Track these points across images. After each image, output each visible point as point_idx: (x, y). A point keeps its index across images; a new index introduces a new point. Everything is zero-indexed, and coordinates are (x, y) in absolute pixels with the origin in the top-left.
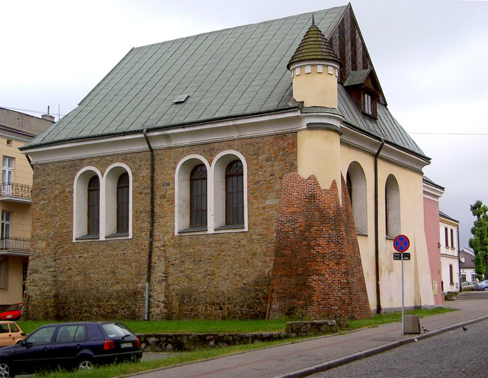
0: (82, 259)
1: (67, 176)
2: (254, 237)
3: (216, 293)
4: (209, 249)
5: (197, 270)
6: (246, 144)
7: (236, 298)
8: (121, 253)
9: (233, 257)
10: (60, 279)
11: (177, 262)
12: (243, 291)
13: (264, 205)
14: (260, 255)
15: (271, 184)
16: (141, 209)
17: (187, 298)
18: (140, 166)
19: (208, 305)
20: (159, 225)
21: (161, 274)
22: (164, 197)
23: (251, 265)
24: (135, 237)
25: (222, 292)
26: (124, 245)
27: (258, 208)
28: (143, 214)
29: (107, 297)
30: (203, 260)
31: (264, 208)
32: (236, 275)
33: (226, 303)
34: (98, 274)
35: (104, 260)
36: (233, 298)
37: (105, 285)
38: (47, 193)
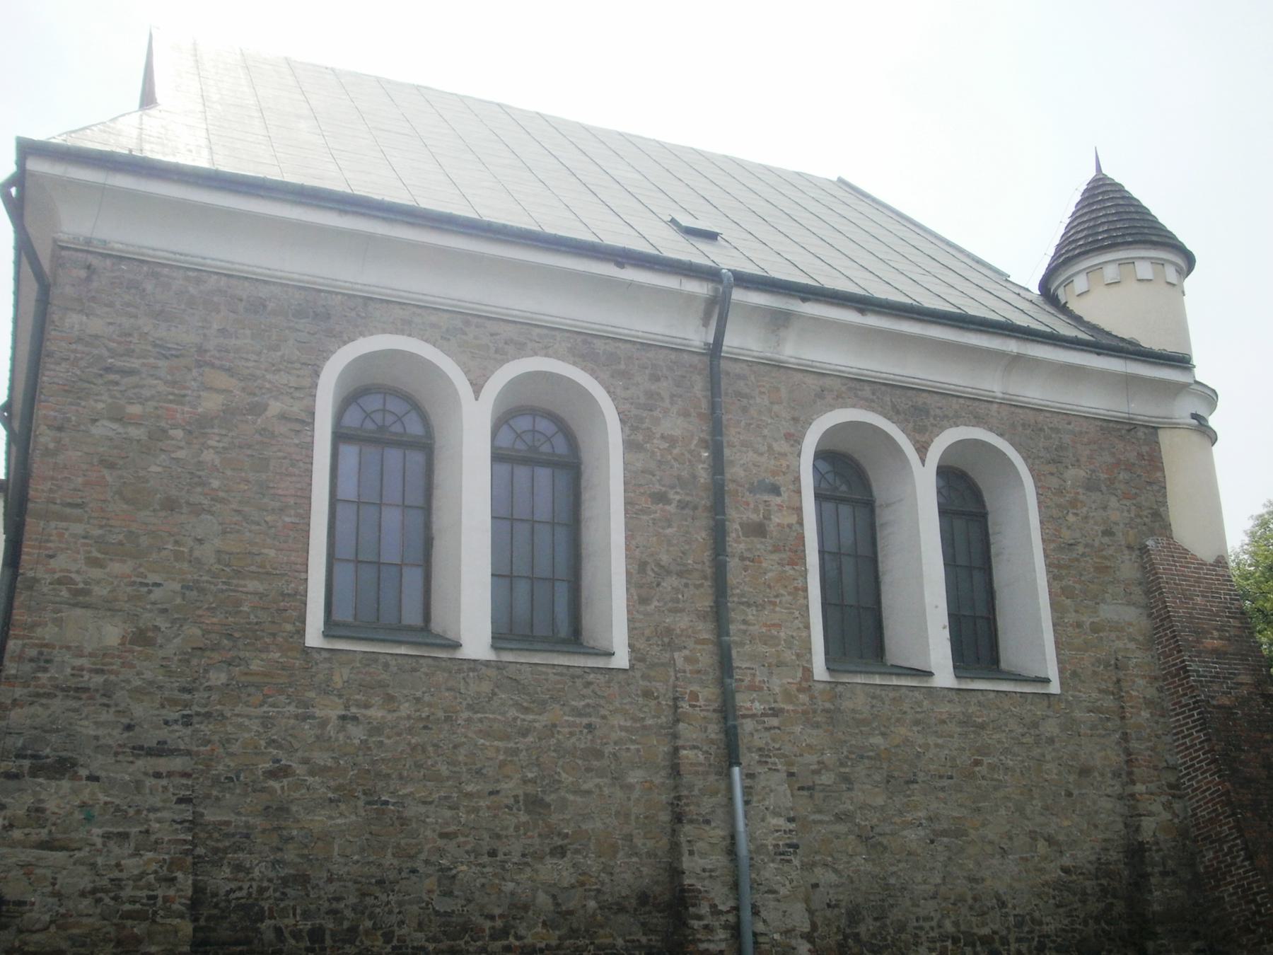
0: (357, 733)
1: (276, 348)
2: (1077, 714)
3: (975, 899)
4: (940, 741)
5: (901, 813)
6: (1029, 426)
7: (1044, 920)
8: (573, 725)
9: (1022, 774)
11: (826, 778)
12: (1065, 893)
13: (1096, 620)
14: (1102, 775)
15: (1106, 558)
16: (665, 559)
17: (870, 921)
18: (650, 395)
19: (949, 943)
20: (745, 632)
21: (780, 822)
22: (758, 530)
23: (1078, 806)
24: (639, 665)
25: (998, 897)
26: (585, 691)
27: (1079, 625)
28: (670, 582)
29: (497, 911)
30: (921, 777)
31: (1095, 628)
32: (1033, 836)
33: (1012, 938)
34: (453, 807)
35: (484, 748)
36: (1033, 920)
37: (486, 859)
38: (146, 393)
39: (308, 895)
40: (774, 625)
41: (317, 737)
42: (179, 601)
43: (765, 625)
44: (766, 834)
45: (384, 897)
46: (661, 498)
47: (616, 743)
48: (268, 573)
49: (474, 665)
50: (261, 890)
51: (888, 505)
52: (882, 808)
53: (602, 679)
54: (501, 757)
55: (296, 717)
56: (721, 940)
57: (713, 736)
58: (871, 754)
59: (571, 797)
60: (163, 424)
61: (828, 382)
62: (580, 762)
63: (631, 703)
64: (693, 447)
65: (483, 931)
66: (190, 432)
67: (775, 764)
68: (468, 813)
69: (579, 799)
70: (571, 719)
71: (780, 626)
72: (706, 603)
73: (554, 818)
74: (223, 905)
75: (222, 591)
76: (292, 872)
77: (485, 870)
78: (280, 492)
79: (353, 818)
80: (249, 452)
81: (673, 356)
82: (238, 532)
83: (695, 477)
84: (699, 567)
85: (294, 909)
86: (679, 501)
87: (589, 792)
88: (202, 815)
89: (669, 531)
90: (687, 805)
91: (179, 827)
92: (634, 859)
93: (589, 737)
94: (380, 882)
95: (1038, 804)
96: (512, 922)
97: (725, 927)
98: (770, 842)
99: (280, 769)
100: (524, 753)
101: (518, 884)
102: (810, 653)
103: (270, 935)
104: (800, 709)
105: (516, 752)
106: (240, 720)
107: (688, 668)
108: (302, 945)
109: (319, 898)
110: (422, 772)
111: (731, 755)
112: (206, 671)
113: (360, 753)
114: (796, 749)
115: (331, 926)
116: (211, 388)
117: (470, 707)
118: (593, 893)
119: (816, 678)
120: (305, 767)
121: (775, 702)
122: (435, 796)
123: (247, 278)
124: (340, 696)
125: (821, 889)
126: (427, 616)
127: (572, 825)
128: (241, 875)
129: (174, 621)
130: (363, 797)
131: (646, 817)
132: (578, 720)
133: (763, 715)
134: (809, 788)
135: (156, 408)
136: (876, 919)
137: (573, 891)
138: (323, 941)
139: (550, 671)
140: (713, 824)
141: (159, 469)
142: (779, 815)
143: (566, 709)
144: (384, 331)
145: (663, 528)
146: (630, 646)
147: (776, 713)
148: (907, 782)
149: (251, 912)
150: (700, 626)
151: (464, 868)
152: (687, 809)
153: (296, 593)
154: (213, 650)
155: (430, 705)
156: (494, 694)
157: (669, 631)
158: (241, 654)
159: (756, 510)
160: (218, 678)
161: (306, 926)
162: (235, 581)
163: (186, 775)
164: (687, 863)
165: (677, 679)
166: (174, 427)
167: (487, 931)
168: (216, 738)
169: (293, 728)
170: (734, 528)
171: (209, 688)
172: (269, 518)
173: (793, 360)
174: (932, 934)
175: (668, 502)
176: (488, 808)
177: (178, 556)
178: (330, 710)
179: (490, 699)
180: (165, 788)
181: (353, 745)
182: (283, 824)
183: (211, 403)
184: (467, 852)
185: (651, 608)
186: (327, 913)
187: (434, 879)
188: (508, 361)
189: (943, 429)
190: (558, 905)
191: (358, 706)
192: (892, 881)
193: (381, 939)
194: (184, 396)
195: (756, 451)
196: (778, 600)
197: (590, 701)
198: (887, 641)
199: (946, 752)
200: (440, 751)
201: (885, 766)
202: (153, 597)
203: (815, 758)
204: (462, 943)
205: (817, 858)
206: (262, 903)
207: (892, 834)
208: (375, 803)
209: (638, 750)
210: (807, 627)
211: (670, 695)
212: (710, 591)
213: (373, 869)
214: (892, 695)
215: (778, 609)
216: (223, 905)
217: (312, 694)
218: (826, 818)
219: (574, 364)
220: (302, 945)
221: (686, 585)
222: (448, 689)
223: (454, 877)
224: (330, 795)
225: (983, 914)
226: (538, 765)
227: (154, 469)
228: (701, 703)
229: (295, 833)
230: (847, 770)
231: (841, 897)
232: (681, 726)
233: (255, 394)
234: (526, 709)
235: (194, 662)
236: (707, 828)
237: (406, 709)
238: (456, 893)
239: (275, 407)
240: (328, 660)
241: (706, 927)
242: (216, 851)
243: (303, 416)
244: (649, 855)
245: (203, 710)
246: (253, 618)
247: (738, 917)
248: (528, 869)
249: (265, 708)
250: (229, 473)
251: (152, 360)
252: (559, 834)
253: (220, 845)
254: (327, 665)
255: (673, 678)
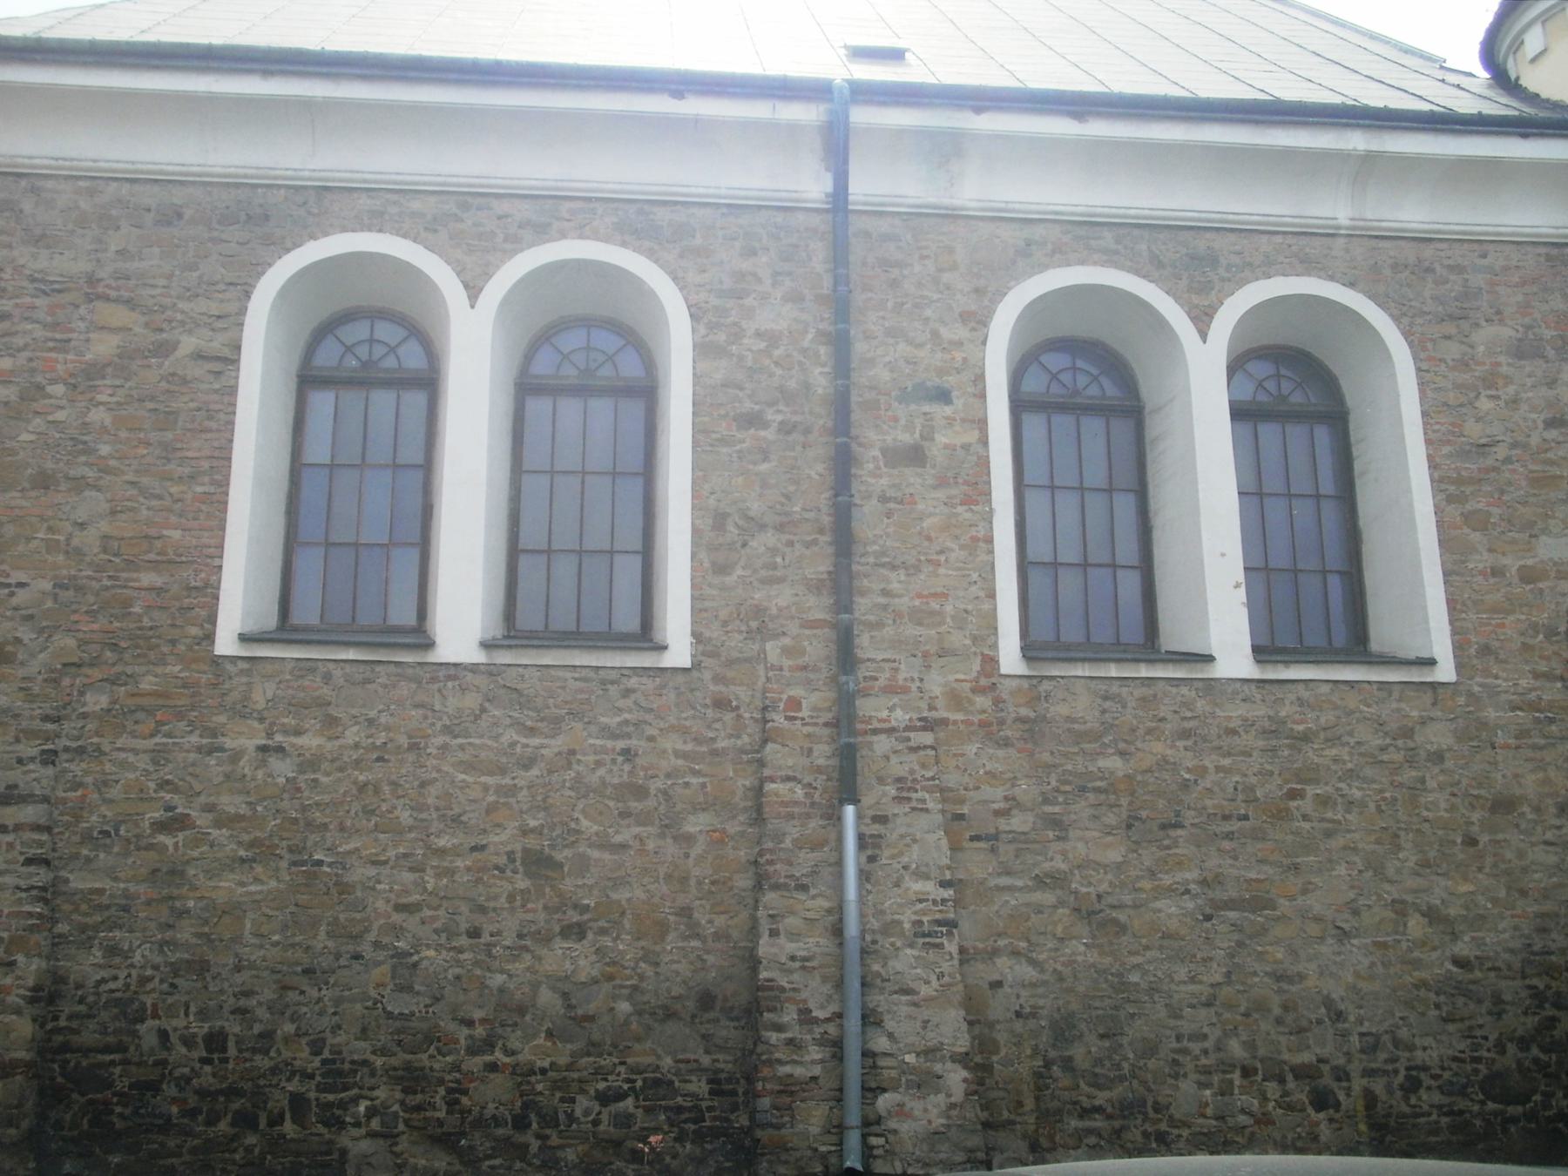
0: (282, 768)
1: (193, 267)
2: (1491, 714)
3: (1286, 1008)
4: (1226, 762)
5: (1152, 874)
7: (1417, 1041)
8: (604, 750)
9: (1379, 810)
10: (78, 881)
11: (1019, 822)
12: (1460, 1001)
13: (1530, 562)
14: (1537, 810)
15: (1552, 463)
16: (755, 507)
17: (1092, 1039)
18: (741, 276)
19: (1236, 1077)
20: (885, 607)
21: (929, 887)
22: (915, 456)
23: (1489, 860)
24: (707, 662)
25: (1328, 1003)
26: (621, 703)
27: (1497, 572)
29: (478, 1014)
30: (1190, 817)
31: (1528, 576)
32: (1400, 909)
33: (1355, 1068)
34: (418, 869)
35: (465, 786)
36: (1397, 1043)
37: (463, 941)
38: (19, 341)
39: (206, 988)
40: (935, 595)
41: (227, 776)
42: (49, 604)
43: (919, 596)
44: (901, 905)
45: (314, 993)
46: (752, 420)
47: (668, 776)
48: (170, 562)
49: (455, 670)
50: (144, 980)
51: (1160, 408)
52: (1119, 866)
53: (650, 684)
54: (491, 798)
55: (199, 749)
56: (813, 1062)
57: (821, 762)
58: (1099, 784)
59: (595, 854)
60: (39, 379)
61: (1039, 232)
62: (611, 804)
63: (694, 717)
64: (806, 344)
65: (457, 1041)
66: (75, 386)
67: (924, 801)
68: (438, 876)
69: (607, 856)
70: (598, 742)
71: (945, 596)
72: (820, 565)
73: (568, 885)
74: (91, 999)
75: (107, 588)
76: (186, 956)
77: (462, 957)
78: (190, 454)
79: (273, 884)
80: (151, 405)
81: (779, 218)
82: (132, 509)
83: (807, 386)
84: (811, 515)
85: (187, 1008)
86: (781, 423)
87: (624, 847)
88: (67, 881)
89: (764, 467)
90: (771, 863)
91: (24, 895)
92: (695, 943)
93: (627, 767)
94: (308, 972)
95: (1409, 857)
96: (499, 1031)
97: (822, 1042)
98: (907, 918)
99: (174, 819)
100: (525, 792)
101: (510, 976)
102: (996, 634)
103: (150, 1040)
104: (975, 719)
105: (513, 790)
106: (123, 755)
107: (787, 663)
108: (196, 1055)
109: (222, 991)
110: (374, 820)
111: (847, 787)
112: (82, 693)
113: (286, 796)
114: (966, 779)
115: (237, 1029)
116: (102, 328)
117: (447, 730)
118: (625, 992)
119: (1003, 671)
120: (210, 816)
121: (931, 708)
122: (391, 853)
123: (156, 181)
124: (261, 720)
125: (1007, 989)
126: (422, 612)
127: (595, 892)
128: (117, 960)
129: (41, 631)
130: (287, 856)
131: (713, 883)
132: (609, 744)
133: (907, 728)
134: (988, 838)
135: (31, 360)
136: (1102, 1036)
137: (595, 987)
138: (224, 1049)
139: (568, 675)
140: (813, 892)
141: (33, 437)
142: (927, 877)
143: (593, 728)
144: (344, 229)
145: (755, 463)
146: (693, 634)
147: (928, 725)
148: (1163, 827)
149: (129, 1010)
150: (812, 600)
151: (431, 953)
152: (771, 869)
153: (207, 585)
154: (92, 665)
155: (388, 729)
156: (483, 710)
157: (759, 611)
158: (129, 670)
159: (909, 428)
160: (97, 701)
161: (200, 1029)
162: (124, 575)
163: (37, 828)
164: (765, 948)
165: (768, 679)
166: (53, 381)
167: (463, 1041)
168: (89, 780)
169: (193, 765)
170: (870, 457)
171: (84, 716)
172: (173, 490)
173: (974, 204)
174: (1204, 1061)
175: (765, 425)
176: (468, 869)
177: (52, 546)
178: (245, 739)
179: (477, 717)
180: (11, 846)
181: (276, 784)
182: (176, 892)
183: (104, 347)
184: (436, 931)
185: (729, 580)
186: (232, 1013)
187: (386, 968)
188: (522, 250)
189: (1243, 282)
190: (570, 1007)
191: (286, 733)
192: (1134, 978)
193: (307, 1050)
194: (69, 340)
195: (910, 342)
196: (943, 558)
197: (627, 716)
198: (1161, 616)
199: (1237, 778)
200: (400, 792)
201: (1124, 802)
202: (15, 601)
203: (1000, 792)
204: (424, 1057)
205: (1001, 943)
206: (143, 998)
207: (1135, 907)
208: (303, 863)
209: (704, 785)
210: (992, 595)
211: (759, 704)
212: (830, 550)
213: (299, 954)
214: (1138, 693)
215: (942, 571)
216: (91, 999)
217: (222, 719)
218: (1019, 883)
219: (624, 244)
220: (196, 1055)
221: (791, 544)
222: (416, 706)
223: (415, 965)
224: (242, 853)
225: (1301, 1031)
226: (545, 809)
227: (25, 437)
228: (805, 713)
229: (191, 904)
230: (1057, 809)
231: (1041, 1002)
232: (770, 747)
233: (161, 330)
234: (532, 729)
235: (66, 682)
236: (802, 896)
237: (352, 734)
238: (417, 987)
239: (188, 344)
240: (247, 673)
241: (790, 1042)
242: (83, 928)
243: (226, 352)
244: (717, 936)
245: (74, 745)
246: (146, 622)
247: (841, 1026)
248: (528, 957)
249: (157, 740)
250: (123, 434)
251: (28, 300)
252: (575, 906)
253: (88, 920)
254: (244, 680)
255: (763, 679)
